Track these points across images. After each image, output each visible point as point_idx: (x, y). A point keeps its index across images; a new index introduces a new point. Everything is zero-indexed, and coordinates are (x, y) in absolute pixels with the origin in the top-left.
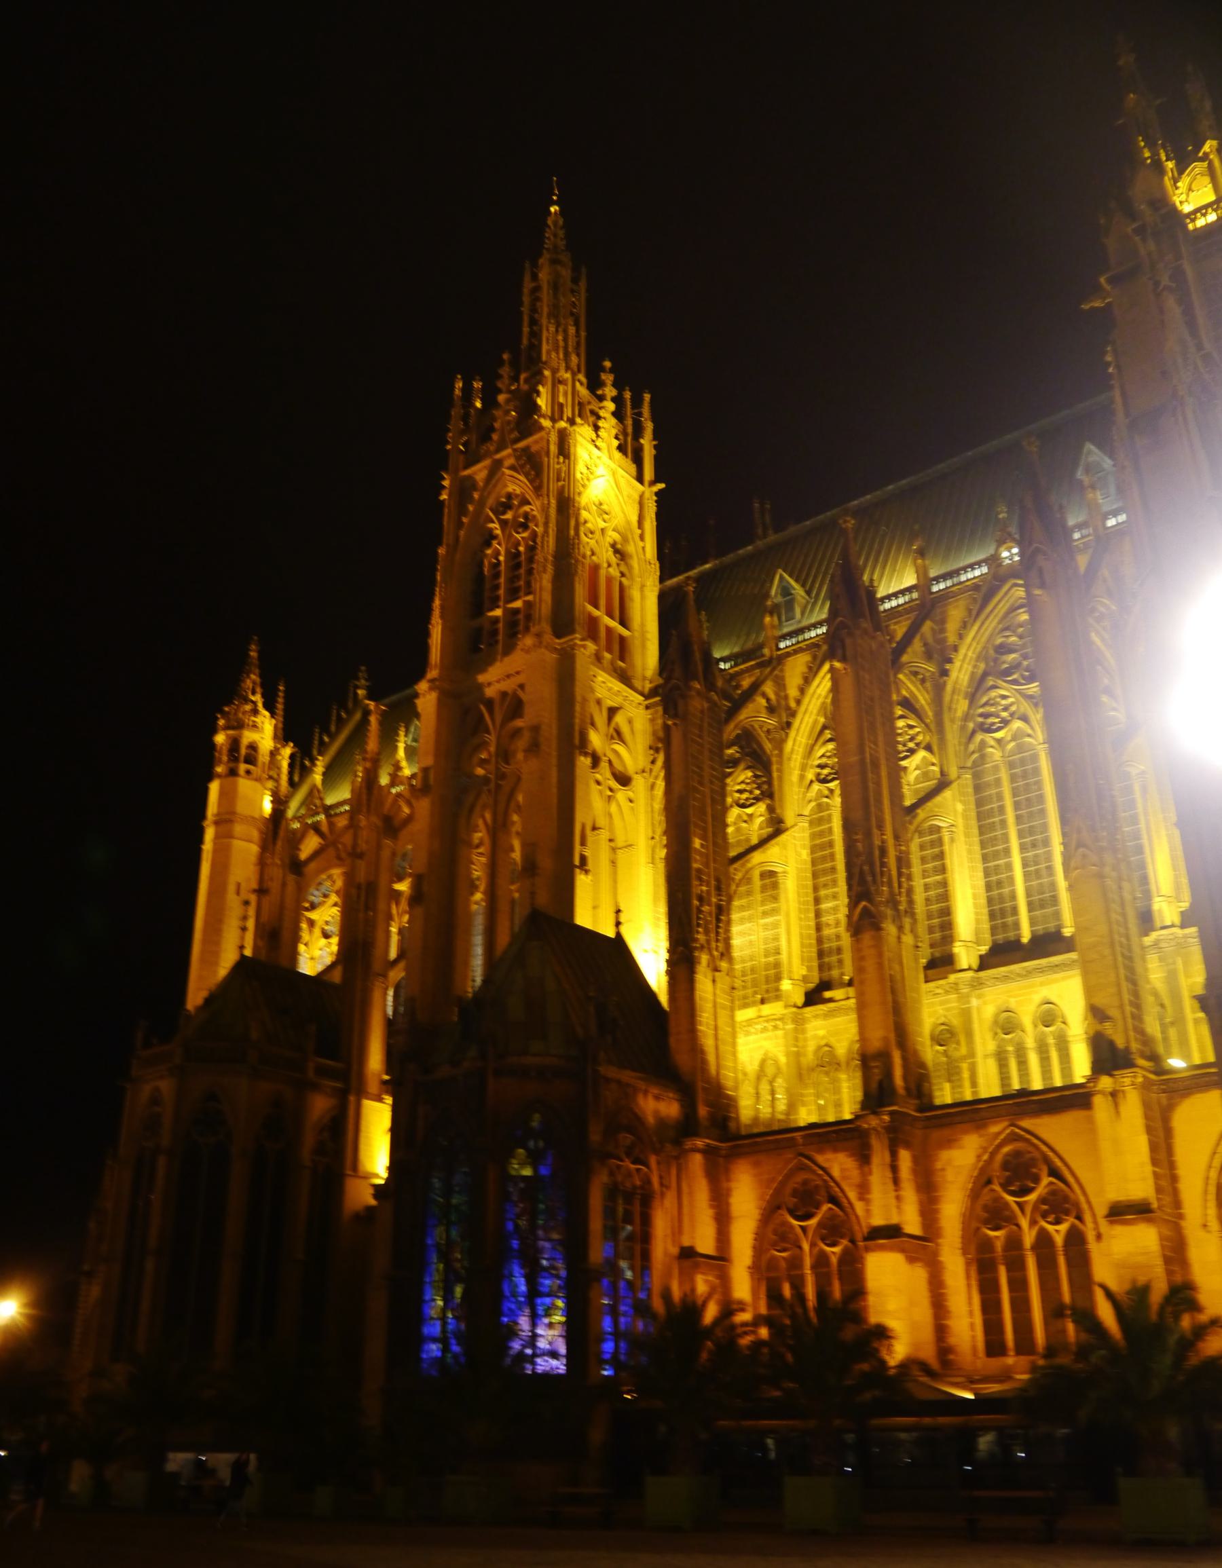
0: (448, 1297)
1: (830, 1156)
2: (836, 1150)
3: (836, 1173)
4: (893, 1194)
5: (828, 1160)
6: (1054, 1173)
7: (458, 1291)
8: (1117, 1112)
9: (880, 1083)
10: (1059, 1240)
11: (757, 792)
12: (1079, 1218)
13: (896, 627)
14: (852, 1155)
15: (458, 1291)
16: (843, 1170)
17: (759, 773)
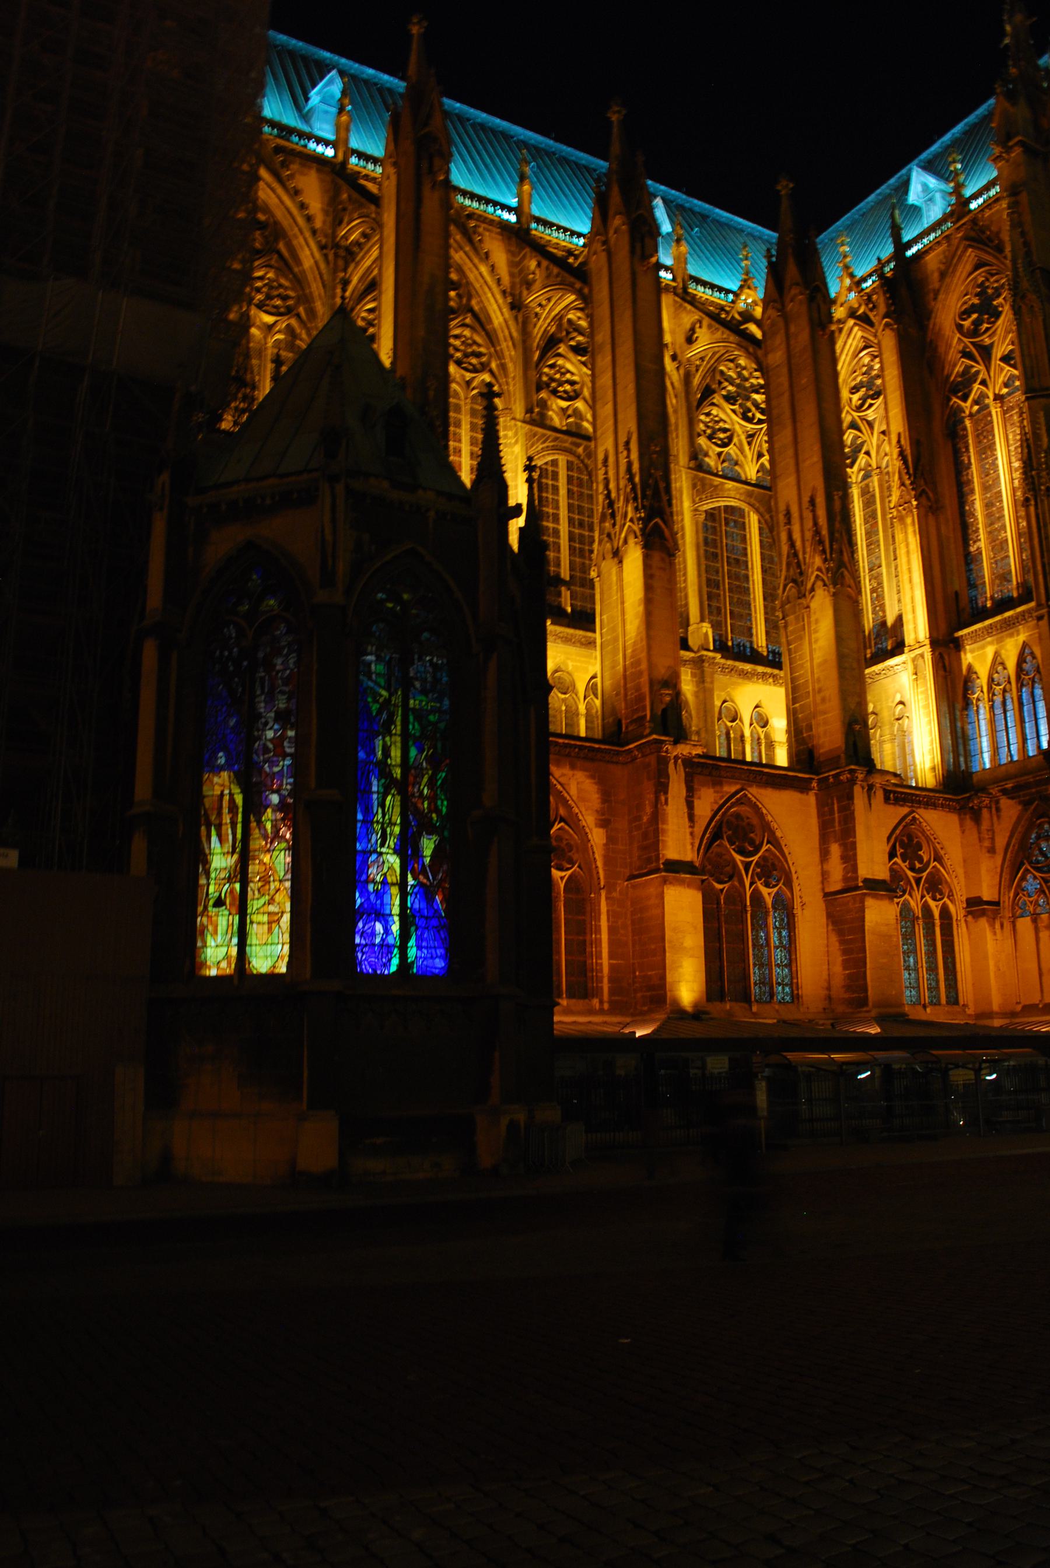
0: (408, 850)
1: (566, 770)
2: (573, 767)
3: (573, 790)
4: (688, 830)
5: (563, 775)
6: (774, 841)
7: (428, 846)
8: (870, 804)
9: (664, 711)
10: (769, 901)
11: (279, 302)
12: (789, 884)
13: (487, 234)
14: (592, 777)
15: (428, 846)
16: (580, 790)
17: (283, 281)
